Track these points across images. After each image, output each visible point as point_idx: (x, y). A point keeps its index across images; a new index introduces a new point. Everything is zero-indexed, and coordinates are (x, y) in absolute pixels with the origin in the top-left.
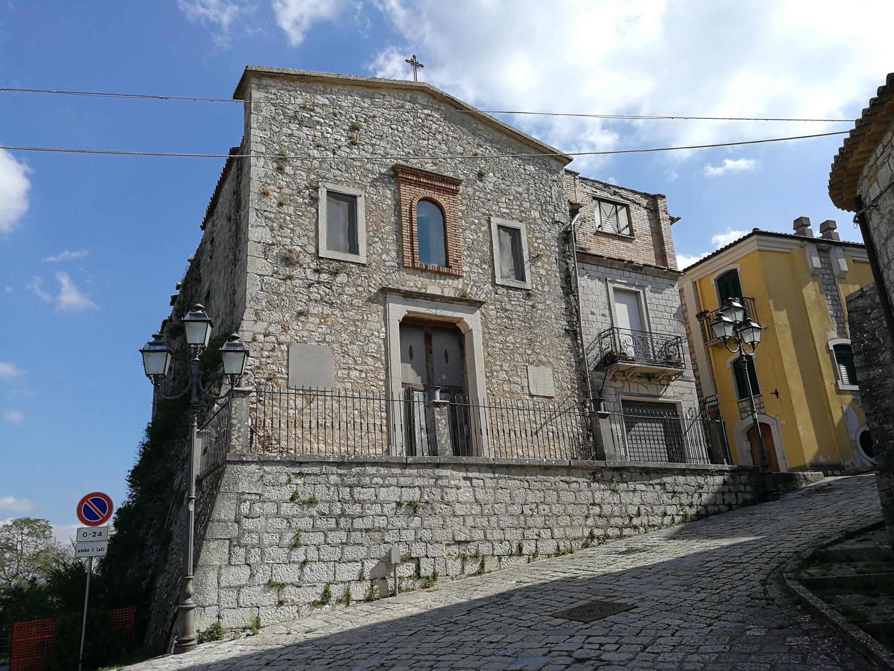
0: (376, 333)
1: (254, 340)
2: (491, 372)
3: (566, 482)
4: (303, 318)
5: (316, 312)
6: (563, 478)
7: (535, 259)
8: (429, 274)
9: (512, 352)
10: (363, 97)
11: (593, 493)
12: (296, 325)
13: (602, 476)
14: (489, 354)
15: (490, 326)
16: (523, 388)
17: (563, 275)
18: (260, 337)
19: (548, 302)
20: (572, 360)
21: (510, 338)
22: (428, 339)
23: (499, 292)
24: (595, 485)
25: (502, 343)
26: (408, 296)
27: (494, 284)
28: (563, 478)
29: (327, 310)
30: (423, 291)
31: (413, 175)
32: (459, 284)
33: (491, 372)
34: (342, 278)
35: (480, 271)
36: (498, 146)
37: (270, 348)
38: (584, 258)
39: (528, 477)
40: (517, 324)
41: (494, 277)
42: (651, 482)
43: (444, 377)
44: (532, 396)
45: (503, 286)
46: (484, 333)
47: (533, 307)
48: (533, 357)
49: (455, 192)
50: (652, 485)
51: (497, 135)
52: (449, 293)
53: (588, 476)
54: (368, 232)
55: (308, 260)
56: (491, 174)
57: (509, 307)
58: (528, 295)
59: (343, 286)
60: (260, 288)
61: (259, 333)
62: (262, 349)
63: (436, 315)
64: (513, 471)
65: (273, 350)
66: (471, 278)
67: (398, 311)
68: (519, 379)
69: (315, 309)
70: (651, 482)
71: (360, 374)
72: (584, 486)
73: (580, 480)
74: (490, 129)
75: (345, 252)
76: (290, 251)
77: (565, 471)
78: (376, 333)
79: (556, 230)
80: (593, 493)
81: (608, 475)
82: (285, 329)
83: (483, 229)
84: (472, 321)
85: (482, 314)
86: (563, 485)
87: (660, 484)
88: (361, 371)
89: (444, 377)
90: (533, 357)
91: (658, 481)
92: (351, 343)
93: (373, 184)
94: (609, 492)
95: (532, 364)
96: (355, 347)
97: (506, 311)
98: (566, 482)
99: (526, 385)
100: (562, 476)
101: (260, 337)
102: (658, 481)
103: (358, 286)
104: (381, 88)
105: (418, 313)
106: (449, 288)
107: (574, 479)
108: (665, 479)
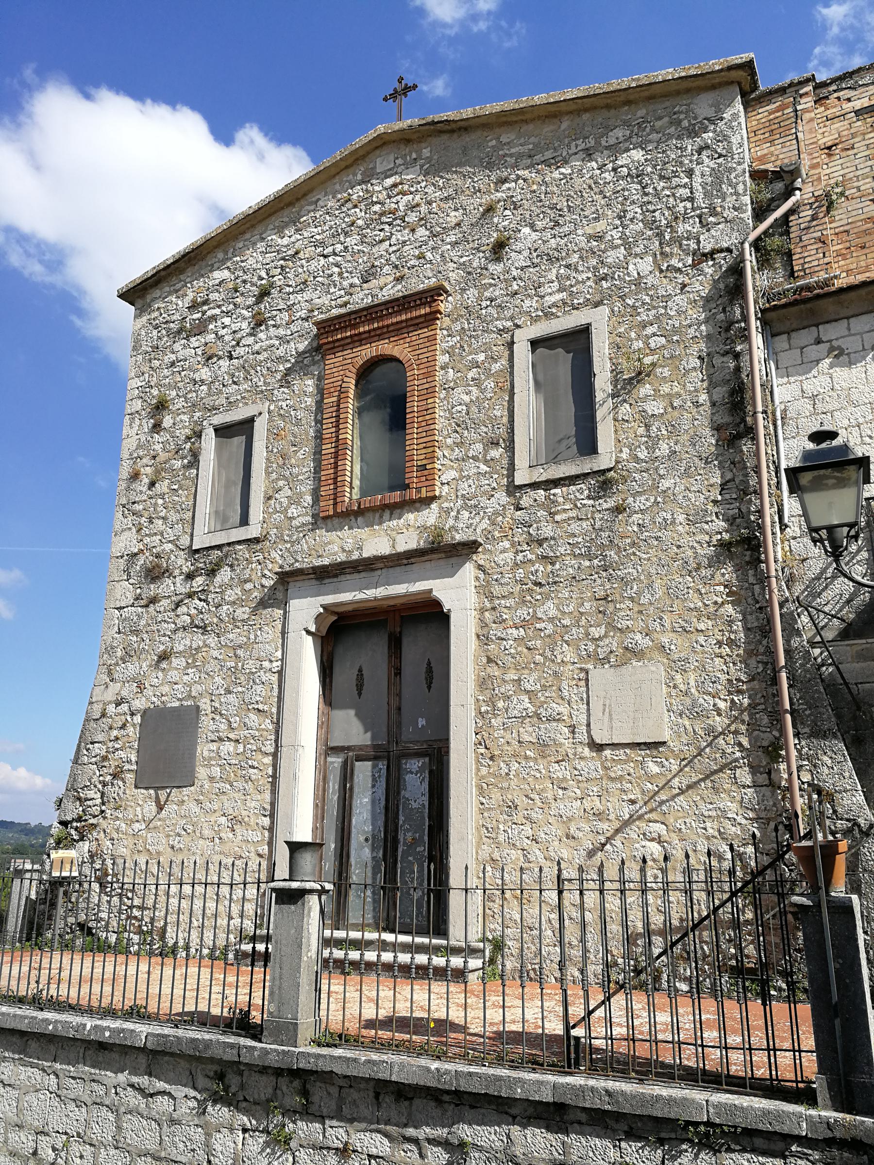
0: (266, 664)
1: (103, 715)
2: (492, 702)
3: (140, 1090)
4: (164, 665)
5: (182, 648)
6: (135, 1079)
7: (626, 385)
8: (370, 515)
9: (552, 641)
10: (280, 232)
11: (208, 1135)
12: (154, 678)
13: (242, 1087)
14: (490, 660)
15: (497, 590)
16: (573, 729)
17: (720, 393)
18: (111, 709)
19: (666, 484)
20: (738, 626)
21: (550, 608)
22: (395, 645)
23: (525, 501)
24: (219, 1113)
25: (524, 624)
26: (325, 575)
27: (513, 489)
28: (135, 1079)
29: (198, 639)
30: (355, 556)
31: (343, 329)
32: (430, 516)
33: (492, 702)
34: (224, 575)
35: (484, 468)
36: (549, 154)
37: (120, 724)
38: (812, 312)
39: (58, 1066)
40: (569, 566)
41: (512, 468)
42: (411, 1132)
43: (422, 722)
44: (598, 748)
45: (534, 486)
46: (482, 610)
47: (619, 510)
48: (613, 642)
49: (431, 318)
50: (415, 1141)
51: (548, 129)
52: (408, 541)
53: (201, 1082)
54: (268, 474)
55: (180, 562)
56: (526, 230)
57: (547, 530)
58: (604, 482)
59: (224, 588)
60: (116, 629)
61: (110, 702)
62: (111, 728)
63: (376, 599)
64: (33, 1045)
65: (123, 727)
66: (461, 489)
67: (305, 610)
68: (564, 709)
69: (183, 642)
70: (411, 1132)
71: (236, 748)
72: (187, 1107)
73: (179, 1091)
74: (531, 126)
75: (573, 458)
76: (158, 556)
77: (142, 1060)
78: (266, 664)
79: (702, 284)
80: (208, 1135)
81: (262, 1087)
82: (141, 687)
83: (496, 367)
84: (457, 592)
85: (480, 567)
86: (133, 1099)
87: (445, 1144)
88: (237, 741)
89: (422, 722)
90: (613, 642)
91: (441, 1132)
92: (229, 692)
93: (285, 381)
94: (262, 1139)
95: (604, 661)
96: (231, 698)
97: (540, 542)
98: (140, 1090)
99: (583, 719)
100: (134, 1072)
101: (111, 709)
102: (441, 1132)
103: (246, 581)
104: (311, 191)
105: (398, 597)
106: (404, 533)
107: (161, 1085)
108: (465, 1132)
